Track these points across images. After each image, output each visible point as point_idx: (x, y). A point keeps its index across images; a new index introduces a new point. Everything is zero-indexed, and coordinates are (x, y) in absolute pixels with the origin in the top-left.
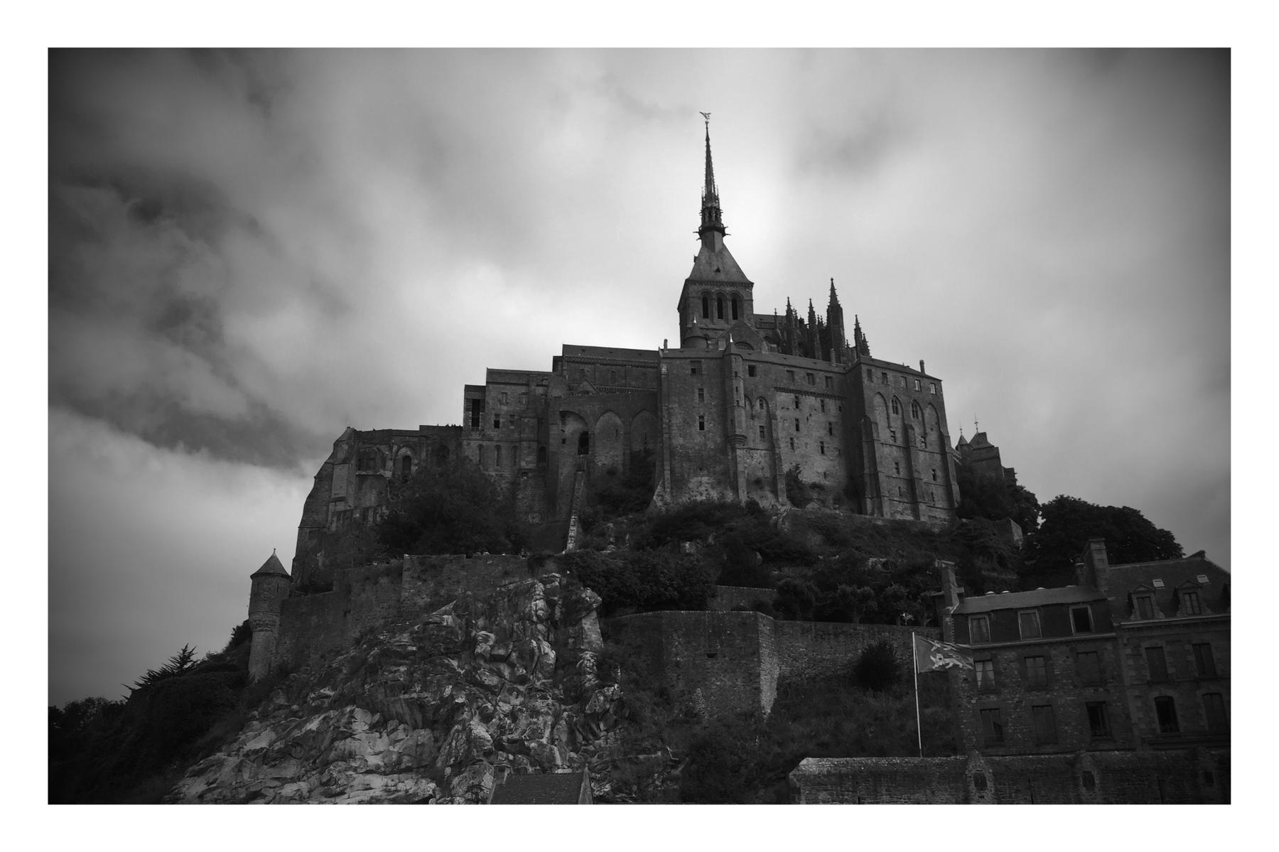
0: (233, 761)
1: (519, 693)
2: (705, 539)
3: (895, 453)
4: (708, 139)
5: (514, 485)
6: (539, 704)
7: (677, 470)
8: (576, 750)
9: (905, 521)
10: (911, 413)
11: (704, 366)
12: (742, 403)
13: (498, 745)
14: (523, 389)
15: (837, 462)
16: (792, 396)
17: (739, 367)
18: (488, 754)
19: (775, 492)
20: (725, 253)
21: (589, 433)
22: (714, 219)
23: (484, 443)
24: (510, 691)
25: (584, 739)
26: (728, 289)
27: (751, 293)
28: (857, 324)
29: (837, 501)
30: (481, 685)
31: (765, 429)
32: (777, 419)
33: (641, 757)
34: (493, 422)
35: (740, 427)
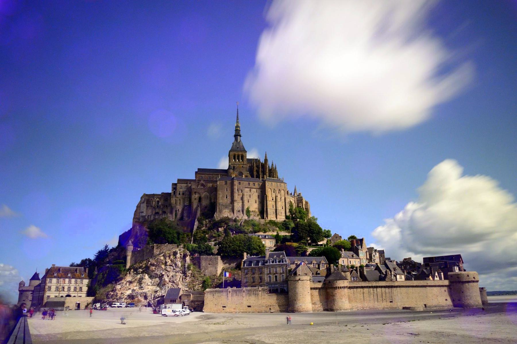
0: (125, 282)
1: (174, 272)
5: (183, 210)
7: (220, 208)
8: (183, 282)
9: (273, 220)
10: (278, 193)
11: (228, 182)
12: (236, 192)
13: (170, 281)
14: (186, 185)
16: (249, 189)
17: (236, 183)
18: (168, 283)
19: (243, 213)
20: (240, 142)
22: (238, 133)
24: (173, 271)
25: (185, 280)
26: (240, 153)
27: (246, 154)
28: (272, 163)
32: (244, 195)
33: (194, 283)
34: (178, 194)
35: (235, 198)
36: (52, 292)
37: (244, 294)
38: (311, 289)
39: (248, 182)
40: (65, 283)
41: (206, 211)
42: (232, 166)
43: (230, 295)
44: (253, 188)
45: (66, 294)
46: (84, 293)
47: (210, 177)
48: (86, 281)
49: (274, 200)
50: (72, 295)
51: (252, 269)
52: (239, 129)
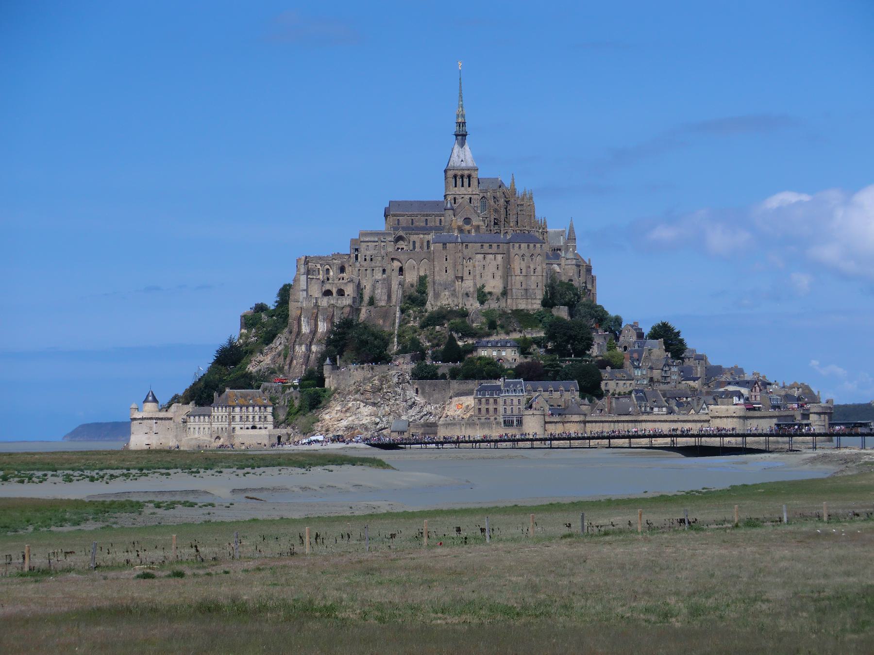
2: (443, 325)
3: (522, 279)
4: (460, 79)
5: (374, 287)
6: (397, 402)
7: (436, 289)
12: (461, 263)
14: (376, 244)
15: (499, 282)
16: (483, 255)
18: (389, 414)
21: (403, 268)
23: (361, 269)
29: (498, 299)
30: (385, 398)
31: (471, 271)
36: (236, 423)
37: (478, 427)
38: (546, 423)
39: (481, 244)
40: (249, 412)
41: (413, 290)
42: (452, 197)
43: (463, 428)
44: (488, 254)
45: (251, 425)
46: (270, 423)
47: (412, 219)
48: (270, 409)
49: (524, 273)
50: (258, 426)
51: (487, 400)
52: (463, 121)
